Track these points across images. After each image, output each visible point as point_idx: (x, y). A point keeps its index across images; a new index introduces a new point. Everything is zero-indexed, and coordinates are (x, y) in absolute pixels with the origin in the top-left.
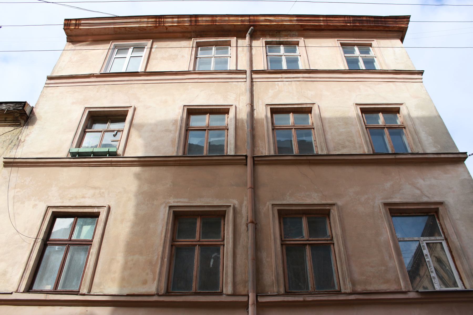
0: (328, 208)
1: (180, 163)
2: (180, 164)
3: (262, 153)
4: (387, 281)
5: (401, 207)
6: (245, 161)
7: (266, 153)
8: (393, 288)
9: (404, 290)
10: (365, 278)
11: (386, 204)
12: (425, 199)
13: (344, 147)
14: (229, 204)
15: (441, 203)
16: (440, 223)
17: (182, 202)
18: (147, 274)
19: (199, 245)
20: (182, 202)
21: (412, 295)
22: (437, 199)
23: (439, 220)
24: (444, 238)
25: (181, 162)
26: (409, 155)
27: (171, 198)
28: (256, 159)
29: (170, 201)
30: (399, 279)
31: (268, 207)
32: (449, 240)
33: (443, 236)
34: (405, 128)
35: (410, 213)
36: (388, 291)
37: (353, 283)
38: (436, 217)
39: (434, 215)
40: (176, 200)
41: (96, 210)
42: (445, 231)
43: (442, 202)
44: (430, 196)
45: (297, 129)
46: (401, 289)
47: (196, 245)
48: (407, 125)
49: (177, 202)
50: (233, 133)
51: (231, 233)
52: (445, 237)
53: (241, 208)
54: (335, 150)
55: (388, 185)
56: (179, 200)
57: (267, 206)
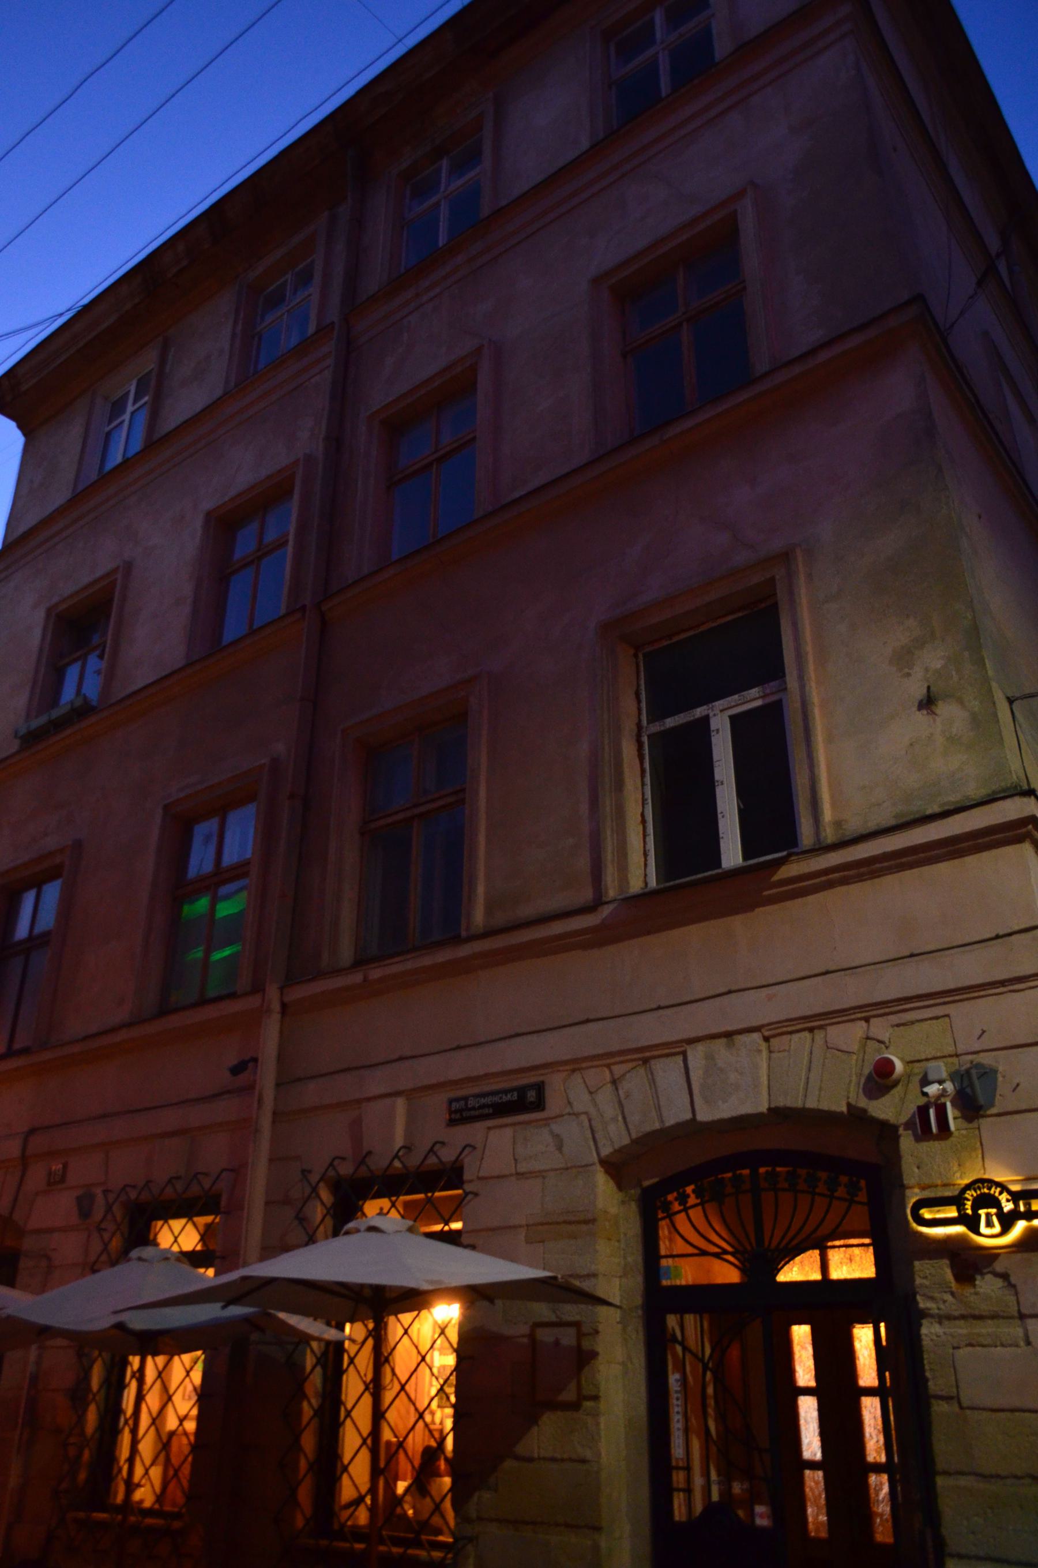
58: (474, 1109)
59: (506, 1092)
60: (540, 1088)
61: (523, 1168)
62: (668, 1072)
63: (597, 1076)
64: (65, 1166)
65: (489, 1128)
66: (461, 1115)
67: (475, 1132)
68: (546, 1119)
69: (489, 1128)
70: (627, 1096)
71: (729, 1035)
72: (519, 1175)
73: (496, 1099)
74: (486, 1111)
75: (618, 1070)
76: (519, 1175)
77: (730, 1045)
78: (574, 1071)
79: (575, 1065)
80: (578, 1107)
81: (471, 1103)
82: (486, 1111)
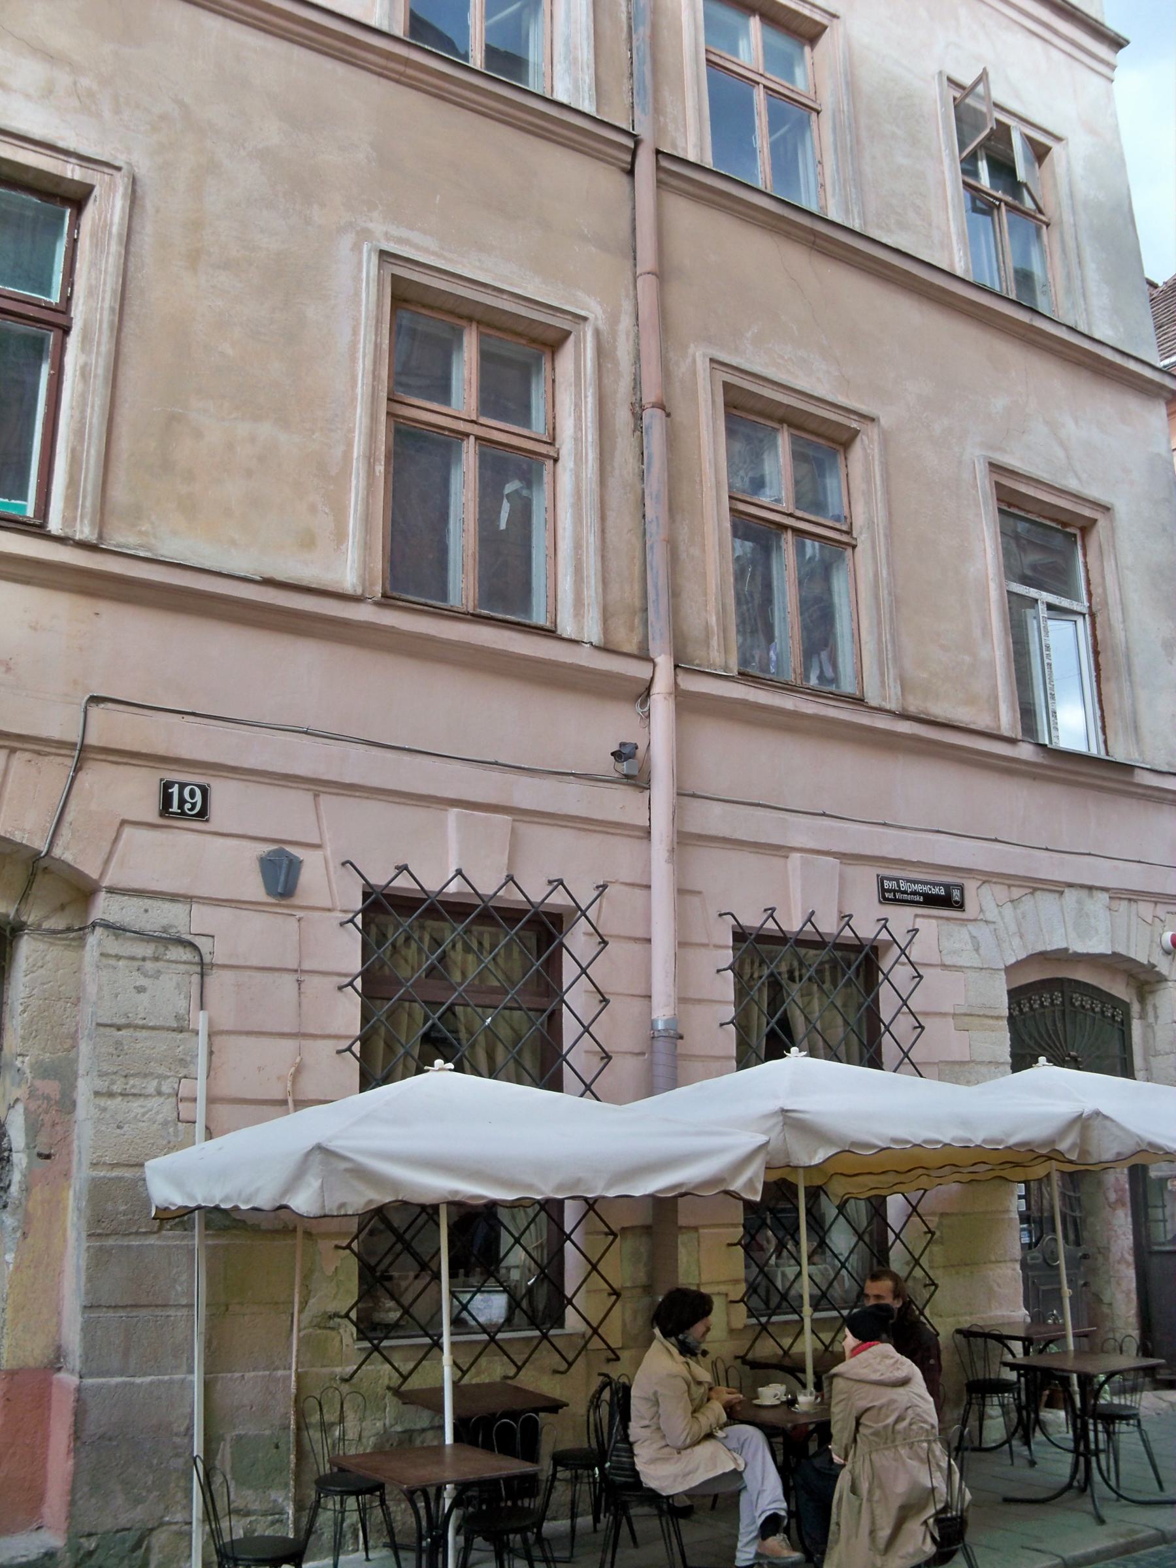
0: (854, 425)
1: (401, 74)
2: (403, 79)
3: (674, 146)
4: (971, 700)
5: (1023, 489)
6: (629, 158)
7: (685, 150)
8: (982, 721)
9: (1006, 731)
10: (925, 675)
11: (995, 467)
12: (1072, 484)
13: (903, 226)
14: (583, 313)
15: (1106, 509)
16: (1086, 564)
17: (417, 247)
18: (313, 509)
19: (477, 438)
20: (417, 247)
21: (1025, 751)
22: (1094, 492)
23: (1085, 555)
24: (1085, 610)
25: (410, 72)
26: (1064, 328)
27: (375, 214)
28: (665, 163)
29: (371, 226)
30: (996, 698)
31: (694, 361)
32: (1098, 620)
33: (1086, 604)
34: (1048, 225)
35: (1028, 512)
36: (972, 726)
37: (905, 685)
38: (1079, 543)
39: (1075, 536)
40: (395, 231)
41: (73, 171)
42: (1097, 590)
43: (1109, 506)
44: (1084, 476)
45: (770, 93)
46: (999, 728)
47: (468, 435)
48: (1062, 222)
49: (400, 241)
50: (584, 18)
51: (589, 424)
52: (1090, 607)
53: (615, 340)
54: (879, 227)
55: (999, 403)
56: (404, 233)
57: (689, 360)
58: (905, 892)
59: (934, 884)
60: (961, 888)
61: (948, 961)
62: (1046, 903)
63: (1001, 892)
64: (205, 791)
65: (916, 916)
66: (895, 895)
67: (902, 918)
68: (963, 920)
69: (916, 916)
70: (1024, 917)
71: (1091, 888)
72: (944, 966)
73: (925, 889)
74: (917, 898)
75: (1016, 893)
76: (944, 966)
77: (1091, 896)
78: (984, 882)
79: (988, 877)
80: (990, 916)
81: (904, 886)
82: (917, 898)
